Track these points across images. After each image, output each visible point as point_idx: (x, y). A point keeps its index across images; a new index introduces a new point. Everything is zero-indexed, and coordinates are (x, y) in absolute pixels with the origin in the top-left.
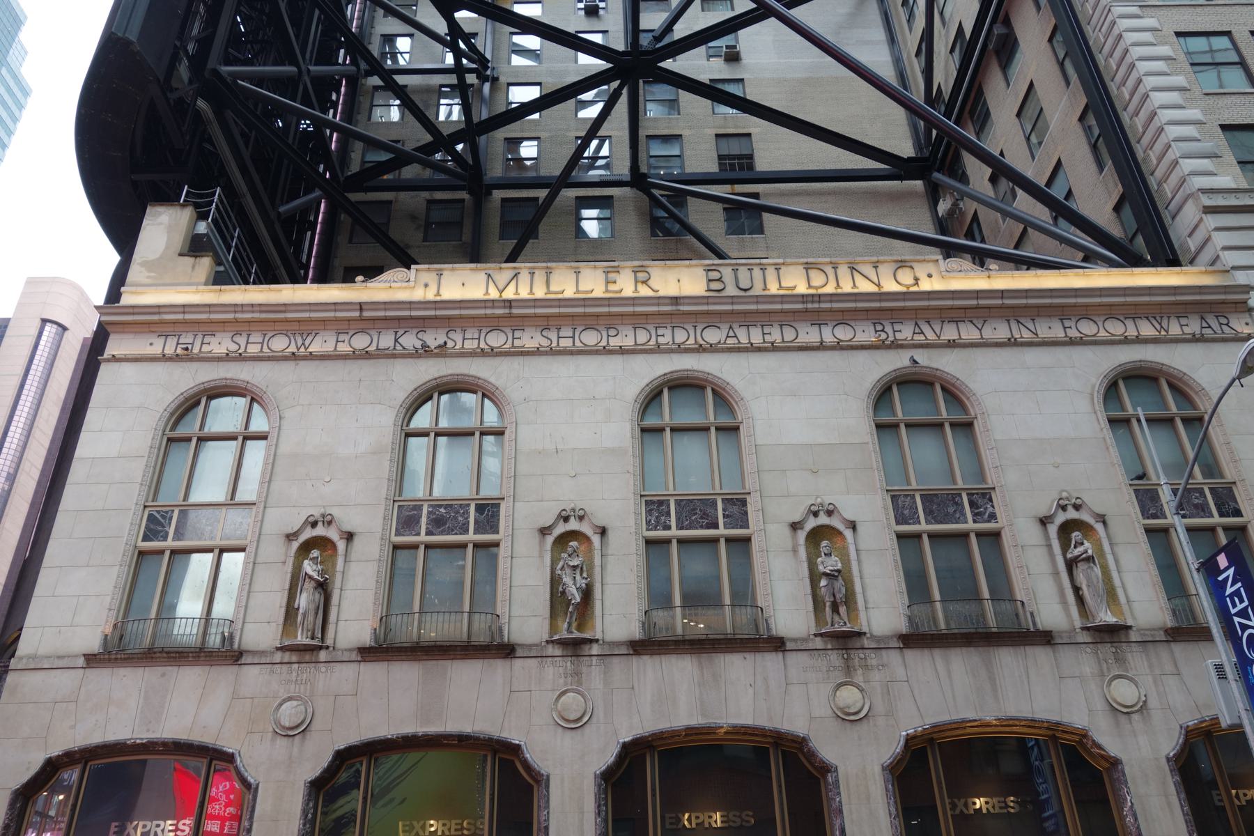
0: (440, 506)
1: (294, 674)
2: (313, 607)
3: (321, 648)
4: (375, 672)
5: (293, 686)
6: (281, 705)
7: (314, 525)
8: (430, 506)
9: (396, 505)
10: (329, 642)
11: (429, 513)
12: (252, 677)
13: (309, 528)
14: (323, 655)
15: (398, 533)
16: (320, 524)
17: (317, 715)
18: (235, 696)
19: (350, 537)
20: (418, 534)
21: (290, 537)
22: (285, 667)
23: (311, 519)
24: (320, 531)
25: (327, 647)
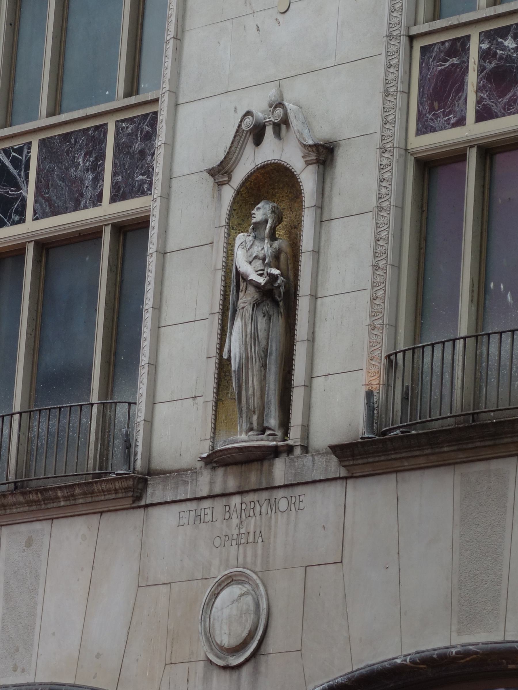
0: (503, 32)
1: (235, 521)
2: (255, 353)
3: (275, 452)
4: (373, 499)
5: (234, 547)
6: (215, 595)
7: (258, 134)
8: (487, 36)
9: (418, 45)
10: (295, 436)
11: (484, 55)
12: (170, 537)
13: (250, 145)
14: (280, 470)
15: (424, 128)
16: (269, 131)
17: (275, 611)
18: (143, 583)
19: (324, 154)
20: (461, 122)
21: (220, 172)
22: (219, 503)
23: (249, 121)
24: (270, 151)
25: (290, 449)
